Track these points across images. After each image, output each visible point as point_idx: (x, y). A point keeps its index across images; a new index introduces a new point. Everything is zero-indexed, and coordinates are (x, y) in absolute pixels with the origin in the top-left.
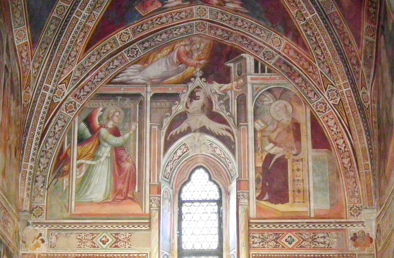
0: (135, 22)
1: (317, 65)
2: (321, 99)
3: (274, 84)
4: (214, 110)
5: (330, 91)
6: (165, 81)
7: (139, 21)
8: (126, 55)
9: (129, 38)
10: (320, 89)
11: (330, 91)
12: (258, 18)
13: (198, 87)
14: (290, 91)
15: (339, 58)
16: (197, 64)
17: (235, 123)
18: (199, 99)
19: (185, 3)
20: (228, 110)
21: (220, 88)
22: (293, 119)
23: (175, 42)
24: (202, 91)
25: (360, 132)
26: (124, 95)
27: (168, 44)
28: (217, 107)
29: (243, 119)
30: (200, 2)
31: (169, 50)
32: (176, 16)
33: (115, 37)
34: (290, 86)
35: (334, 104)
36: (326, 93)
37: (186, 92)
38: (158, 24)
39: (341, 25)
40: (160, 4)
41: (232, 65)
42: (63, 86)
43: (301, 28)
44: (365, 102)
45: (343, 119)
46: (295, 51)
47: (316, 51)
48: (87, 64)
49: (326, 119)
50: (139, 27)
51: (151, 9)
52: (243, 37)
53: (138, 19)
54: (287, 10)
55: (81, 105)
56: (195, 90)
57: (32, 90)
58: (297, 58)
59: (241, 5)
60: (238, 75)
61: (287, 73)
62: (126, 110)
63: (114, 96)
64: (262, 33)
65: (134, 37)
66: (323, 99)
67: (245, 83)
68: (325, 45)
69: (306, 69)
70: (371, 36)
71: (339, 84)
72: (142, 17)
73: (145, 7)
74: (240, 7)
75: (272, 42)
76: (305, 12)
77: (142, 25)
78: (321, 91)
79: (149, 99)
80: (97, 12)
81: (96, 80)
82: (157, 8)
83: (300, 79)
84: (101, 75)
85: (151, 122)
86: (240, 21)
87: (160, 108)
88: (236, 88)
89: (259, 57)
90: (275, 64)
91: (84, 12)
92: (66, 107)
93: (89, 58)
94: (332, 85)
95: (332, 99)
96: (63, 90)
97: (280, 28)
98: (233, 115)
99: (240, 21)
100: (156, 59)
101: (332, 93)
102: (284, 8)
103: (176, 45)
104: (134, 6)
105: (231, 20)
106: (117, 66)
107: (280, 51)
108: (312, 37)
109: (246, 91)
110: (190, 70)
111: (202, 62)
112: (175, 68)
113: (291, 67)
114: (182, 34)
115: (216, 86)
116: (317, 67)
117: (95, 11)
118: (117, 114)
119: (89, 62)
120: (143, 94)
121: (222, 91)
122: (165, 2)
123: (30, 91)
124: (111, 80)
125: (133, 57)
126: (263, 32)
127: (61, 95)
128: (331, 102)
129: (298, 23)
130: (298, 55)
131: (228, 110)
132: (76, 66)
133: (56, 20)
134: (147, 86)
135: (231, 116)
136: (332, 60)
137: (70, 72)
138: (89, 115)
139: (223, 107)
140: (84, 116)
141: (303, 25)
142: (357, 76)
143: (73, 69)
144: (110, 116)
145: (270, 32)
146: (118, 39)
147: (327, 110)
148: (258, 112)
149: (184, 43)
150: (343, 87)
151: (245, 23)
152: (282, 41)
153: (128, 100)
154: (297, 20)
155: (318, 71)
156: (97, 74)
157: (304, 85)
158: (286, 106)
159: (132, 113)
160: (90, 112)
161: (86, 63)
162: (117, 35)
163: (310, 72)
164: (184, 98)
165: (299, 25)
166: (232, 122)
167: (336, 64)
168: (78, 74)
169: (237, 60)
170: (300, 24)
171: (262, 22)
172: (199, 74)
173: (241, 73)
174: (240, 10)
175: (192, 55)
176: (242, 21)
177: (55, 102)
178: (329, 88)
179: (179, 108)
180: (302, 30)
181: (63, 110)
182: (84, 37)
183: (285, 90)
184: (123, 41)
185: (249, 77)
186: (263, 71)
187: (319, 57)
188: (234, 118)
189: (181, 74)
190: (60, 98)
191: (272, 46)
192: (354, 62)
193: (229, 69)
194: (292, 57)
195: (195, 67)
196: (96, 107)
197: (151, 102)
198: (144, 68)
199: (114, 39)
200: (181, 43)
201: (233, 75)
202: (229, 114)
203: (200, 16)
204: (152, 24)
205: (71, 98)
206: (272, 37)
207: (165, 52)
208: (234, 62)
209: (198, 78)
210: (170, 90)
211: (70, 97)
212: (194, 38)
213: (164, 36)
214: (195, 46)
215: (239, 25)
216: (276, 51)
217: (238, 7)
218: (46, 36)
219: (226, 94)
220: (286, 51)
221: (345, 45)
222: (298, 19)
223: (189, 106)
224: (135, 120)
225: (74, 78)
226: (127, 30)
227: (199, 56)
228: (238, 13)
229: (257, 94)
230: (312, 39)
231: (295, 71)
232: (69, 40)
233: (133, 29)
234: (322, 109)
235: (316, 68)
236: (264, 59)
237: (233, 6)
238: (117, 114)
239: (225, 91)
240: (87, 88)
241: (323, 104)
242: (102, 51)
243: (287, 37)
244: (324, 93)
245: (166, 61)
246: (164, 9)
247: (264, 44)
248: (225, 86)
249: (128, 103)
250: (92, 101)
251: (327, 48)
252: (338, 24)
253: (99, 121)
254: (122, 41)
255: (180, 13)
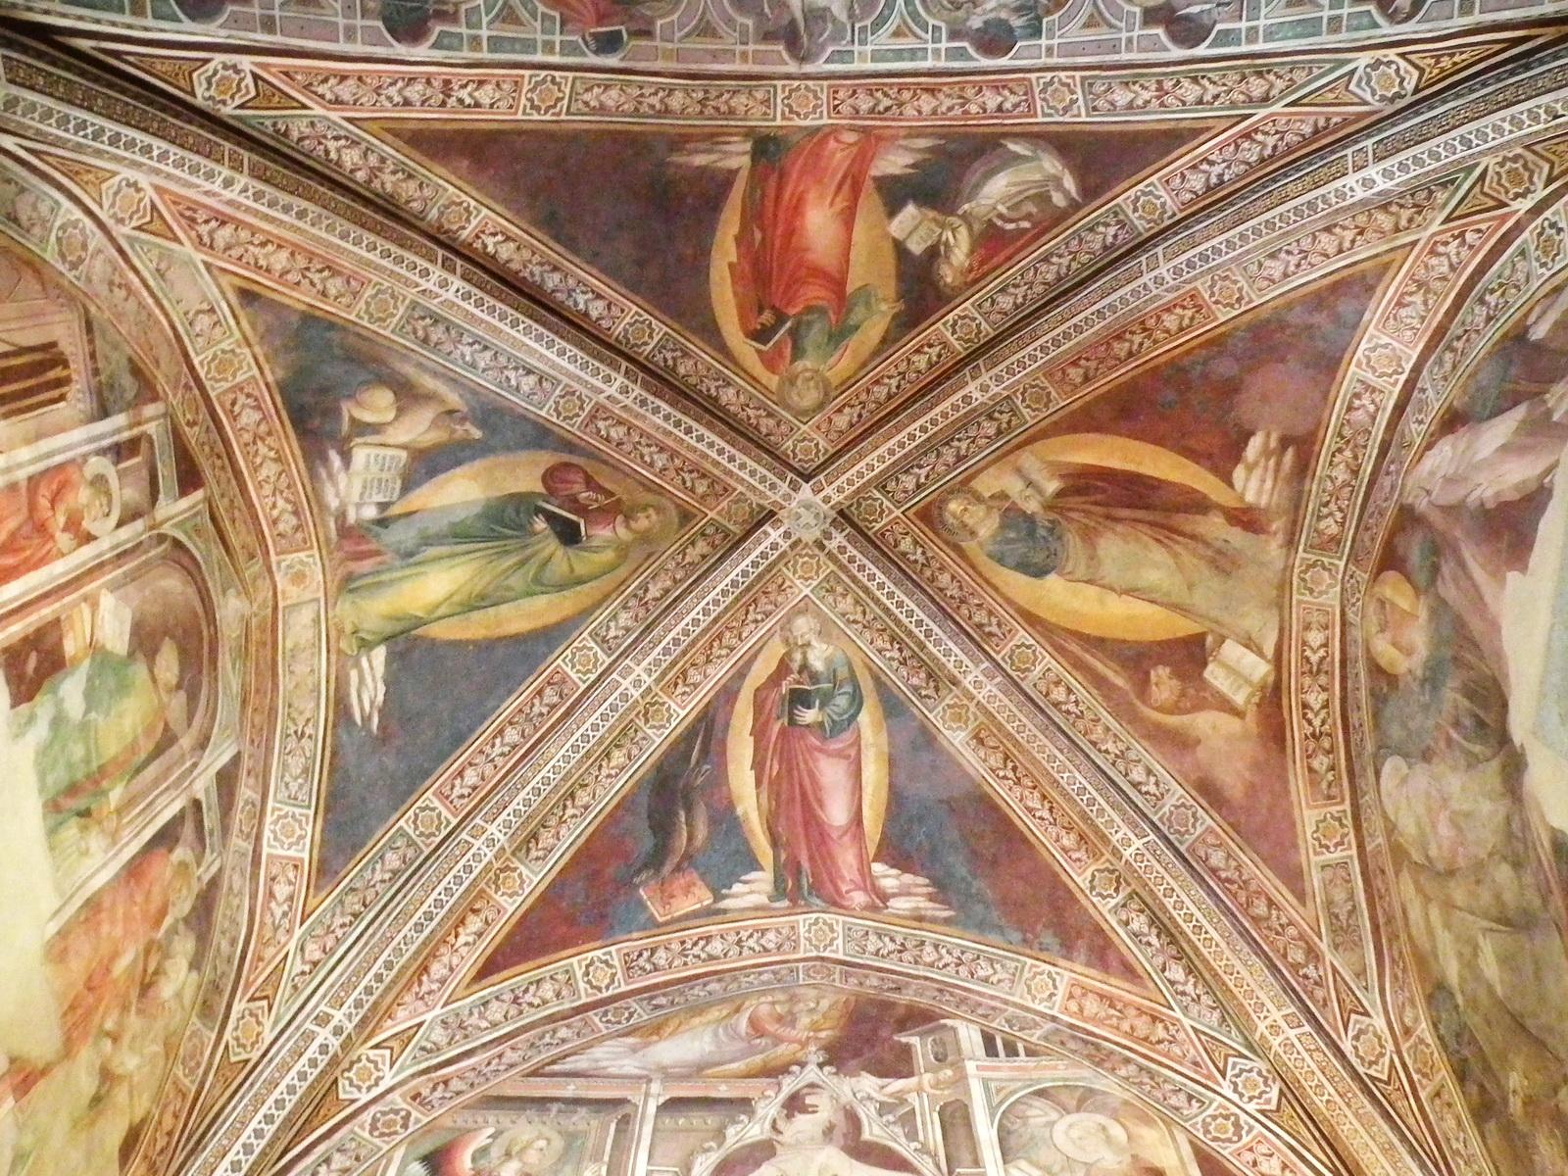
0: (635, 935)
1: (1178, 1014)
2: (1215, 1105)
3: (1054, 1080)
4: (866, 1136)
5: (1237, 1076)
6: (709, 1072)
7: (648, 933)
8: (596, 1020)
9: (613, 981)
10: (1203, 1080)
11: (1237, 1076)
12: (982, 926)
13: (812, 1085)
14: (1104, 1093)
15: (1247, 949)
16: (808, 1038)
17: (939, 1169)
18: (814, 1112)
19: (777, 905)
20: (912, 1135)
21: (883, 1087)
22: (1134, 1157)
23: (746, 996)
24: (826, 1095)
25: (1388, 1150)
26: (577, 1102)
27: (723, 1001)
28: (877, 1130)
29: (967, 1157)
30: (818, 901)
31: (725, 1013)
32: (751, 943)
33: (571, 965)
34: (1106, 1083)
35: (1263, 1112)
36: (1226, 1084)
37: (773, 1094)
38: (698, 957)
39: (1233, 864)
40: (709, 894)
41: (915, 1041)
42: (383, 1056)
43: (1108, 917)
44: (1371, 1063)
45: (1309, 1151)
46: (1102, 996)
47: (1167, 974)
48: (474, 1020)
49: (1248, 1157)
50: (646, 954)
51: (685, 905)
52: (940, 991)
53: (645, 929)
54: (1064, 877)
55: (425, 1120)
56: (805, 1091)
57: (276, 1023)
58: (1110, 1017)
59: (931, 898)
60: (936, 1059)
61: (1089, 1057)
62: (570, 1138)
63: (542, 1103)
64: (995, 973)
65: (627, 984)
66: (1220, 1106)
67: (961, 1079)
68: (1198, 914)
69: (1146, 1039)
70: (1336, 845)
71: (1268, 1022)
72: (659, 925)
73: (667, 898)
74: (931, 905)
75: (1029, 991)
76: (1120, 835)
77: (653, 951)
78: (1210, 1084)
79: (652, 1109)
80: (532, 872)
81: (492, 1068)
82: (698, 906)
83: (1132, 1068)
84: (511, 1056)
85: (649, 1162)
86: (929, 949)
87: (687, 1130)
88: (936, 1085)
89: (994, 1025)
90: (1046, 1038)
91: (492, 828)
92: (375, 1120)
93: (485, 1004)
94: (1242, 1056)
95: (1251, 1099)
96: (378, 1070)
97: (1048, 938)
98: (932, 1148)
99: (929, 949)
100: (682, 1028)
101: (1247, 1079)
102: (1056, 875)
103: (747, 1003)
104: (637, 887)
105: (903, 949)
106: (564, 1041)
107: (1054, 1012)
108: (1145, 935)
109: (967, 1091)
110: (784, 1051)
111: (823, 1035)
112: (740, 1045)
113: (1097, 1047)
114: (763, 983)
115: (868, 1083)
116: (1178, 1020)
117: (526, 866)
118: (542, 1143)
119: (481, 1016)
120: (637, 1098)
121: (891, 1095)
122: (724, 891)
123: (268, 1023)
124: (543, 1067)
125: (619, 1023)
126: (998, 966)
127: (368, 1084)
128: (1251, 1107)
129: (1100, 907)
130: (1112, 1006)
131: (912, 1135)
132: (438, 1011)
133: (408, 846)
134: (650, 1081)
135: (924, 1150)
136: (1228, 953)
137: (417, 1020)
138: (445, 1145)
139: (898, 1130)
140: (427, 1146)
141: (1115, 910)
142: (1319, 993)
143: (428, 1017)
144: (516, 1149)
145: (1018, 961)
146: (579, 974)
147: (1244, 1133)
148: (1013, 1141)
149: (770, 999)
150: (1284, 1025)
151: (944, 951)
152: (1058, 978)
153: (583, 1111)
154: (1095, 900)
155: (1185, 1030)
156: (500, 1056)
157: (1146, 1080)
158: (1104, 1128)
159: (590, 1144)
160: (449, 1137)
161: (471, 1014)
162: (579, 962)
163: (1159, 1042)
164: (769, 1108)
165: (1105, 912)
166: (931, 1166)
167: (1245, 965)
168: (439, 1035)
169: (931, 1031)
170: (1105, 908)
171: (993, 938)
172: (815, 1056)
173: (946, 1056)
174: (929, 913)
175: (793, 1023)
176: (936, 947)
177: (342, 1096)
178: (1233, 1068)
179: (749, 1131)
180: (1115, 925)
181: (362, 1127)
182: (480, 935)
183: (1091, 1091)
184: (593, 987)
185: (970, 1067)
186: (1011, 1051)
187: (1180, 988)
188: (934, 1156)
189: (761, 1056)
190: (364, 1090)
191: (1031, 1005)
192: (1297, 955)
193: (906, 1051)
194: (1093, 1019)
195: (804, 1044)
196: (470, 1125)
197: (656, 1117)
198: (647, 1045)
199: (567, 972)
200: (763, 999)
201: (920, 1061)
202: (919, 1146)
203: (817, 948)
204: (683, 953)
205: (399, 1100)
206: (1026, 975)
207: (715, 1014)
208: (921, 1035)
209: (809, 1067)
210: (723, 1091)
211: (395, 1096)
212: (802, 991)
213: (714, 986)
214: (801, 1005)
215: (928, 960)
216: (1043, 1015)
217: (922, 905)
218: (368, 874)
219: (903, 1101)
220: (1073, 1007)
221: (1255, 920)
222: (1100, 895)
223: (781, 1125)
224: (596, 1157)
225: (424, 1043)
226: (610, 953)
227: (814, 1023)
228: (924, 925)
229: (1001, 1102)
230: (1149, 944)
231: (1112, 1053)
232: (434, 895)
233: (628, 954)
234: (1226, 1132)
235: (1175, 1022)
236: (1011, 1027)
237: (908, 905)
238: (542, 1143)
239: (900, 1099)
240: (456, 1085)
241: (1227, 1118)
242: (528, 998)
243: (1069, 959)
244: (1220, 1085)
245: (716, 1035)
246: (718, 912)
247: (1006, 1002)
248: (898, 1084)
249: (580, 1119)
250: (467, 1114)
251: (1204, 922)
252: (1222, 865)
253: (474, 1159)
254: (589, 982)
255: (764, 932)
